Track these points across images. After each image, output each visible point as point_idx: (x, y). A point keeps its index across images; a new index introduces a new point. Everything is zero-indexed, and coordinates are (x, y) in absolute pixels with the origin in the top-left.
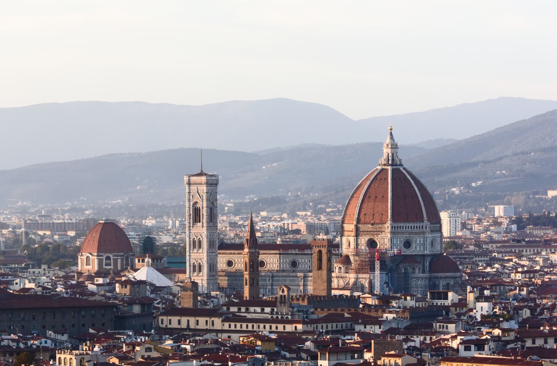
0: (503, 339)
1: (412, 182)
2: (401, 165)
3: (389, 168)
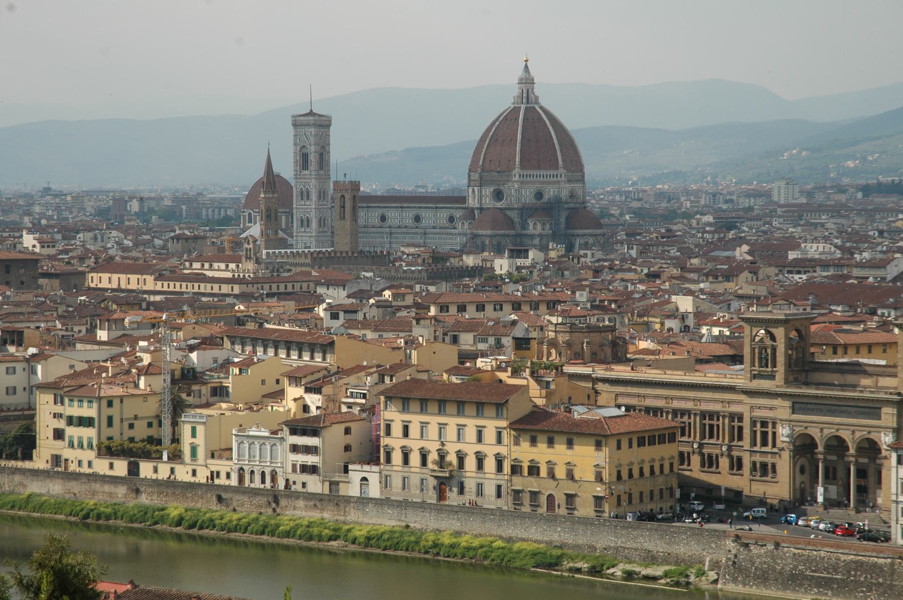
0: (394, 304)
1: (548, 122)
2: (537, 102)
3: (523, 107)
